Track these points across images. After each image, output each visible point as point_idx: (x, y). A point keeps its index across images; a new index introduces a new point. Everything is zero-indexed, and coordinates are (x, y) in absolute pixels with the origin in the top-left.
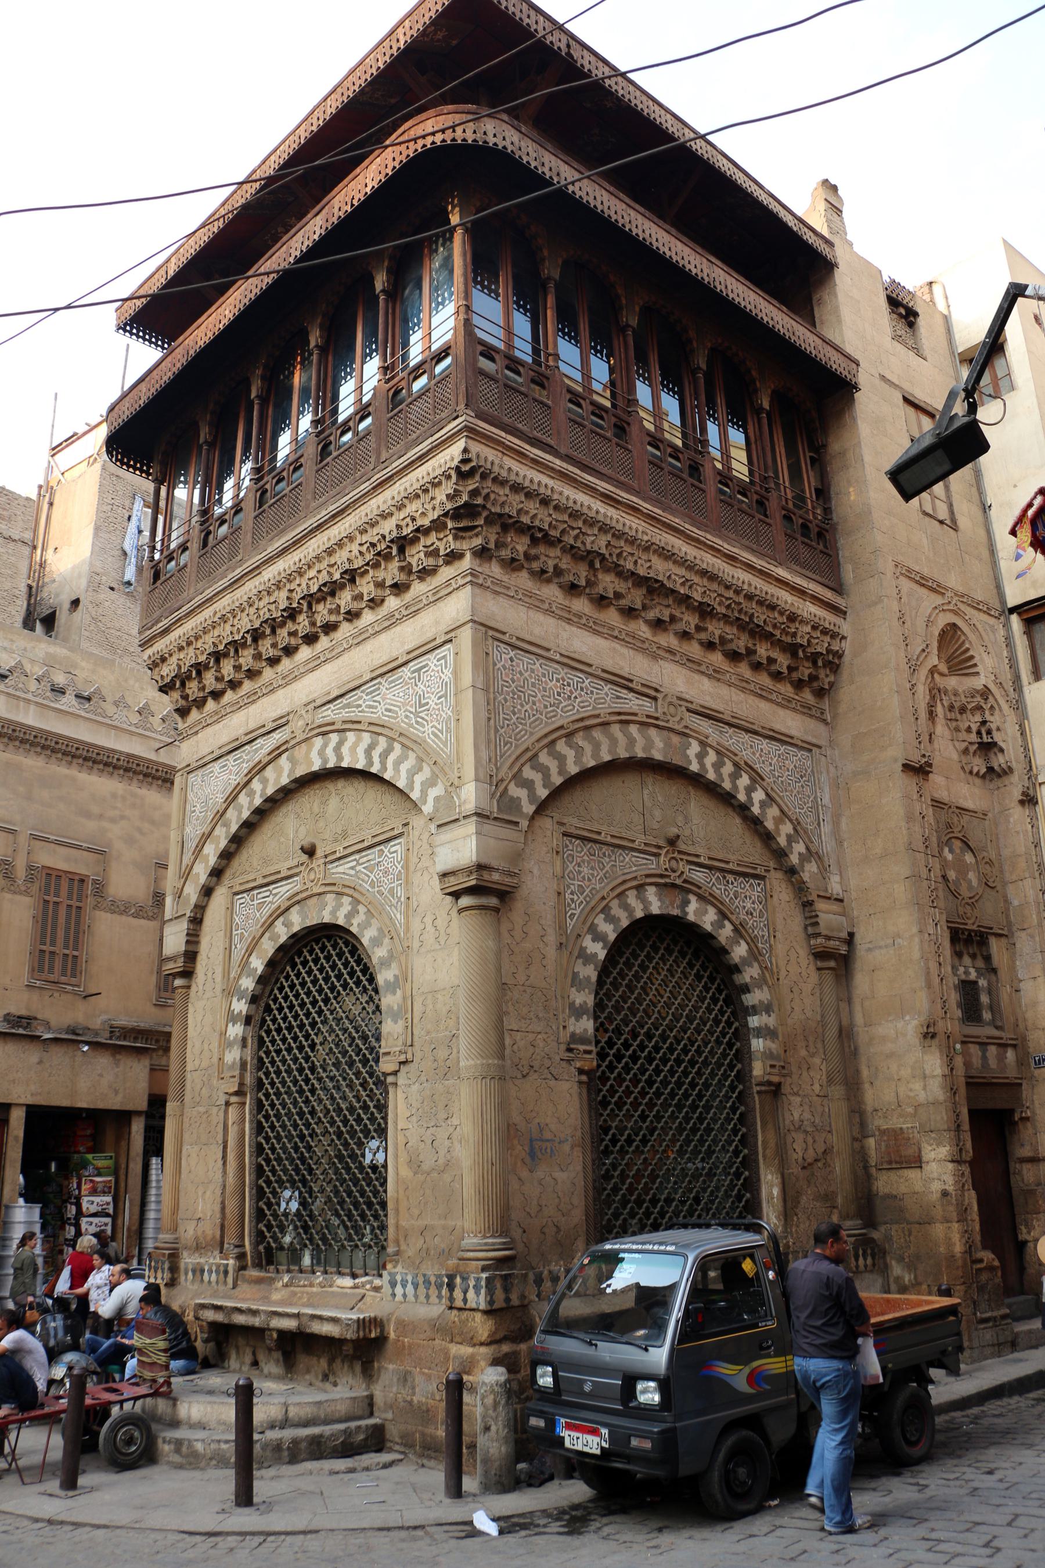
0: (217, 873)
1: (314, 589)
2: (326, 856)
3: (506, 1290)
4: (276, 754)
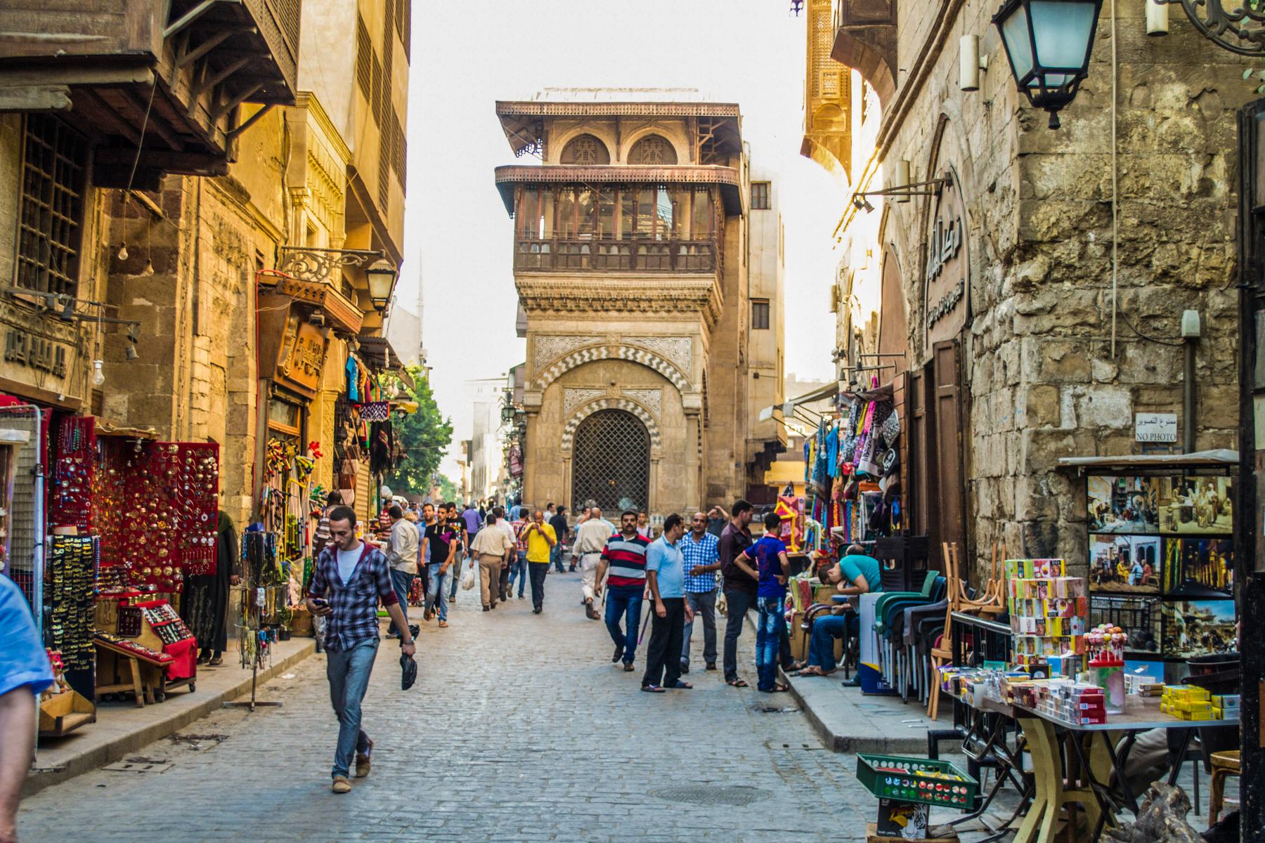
4: (598, 346)
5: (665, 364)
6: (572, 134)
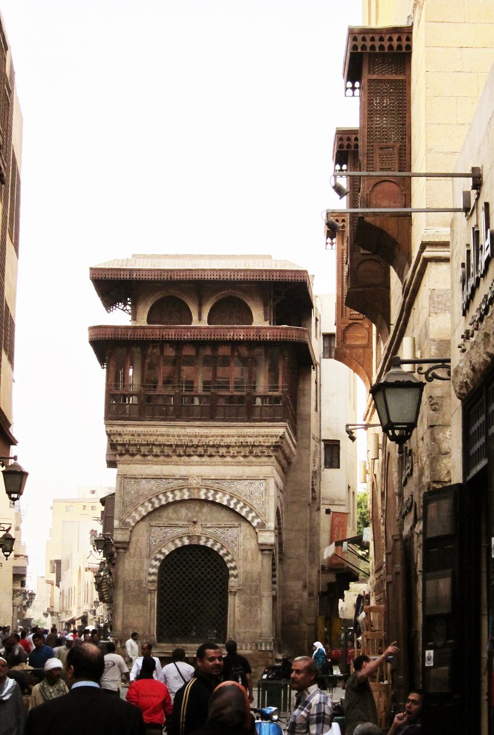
5: (242, 504)
6: (158, 296)
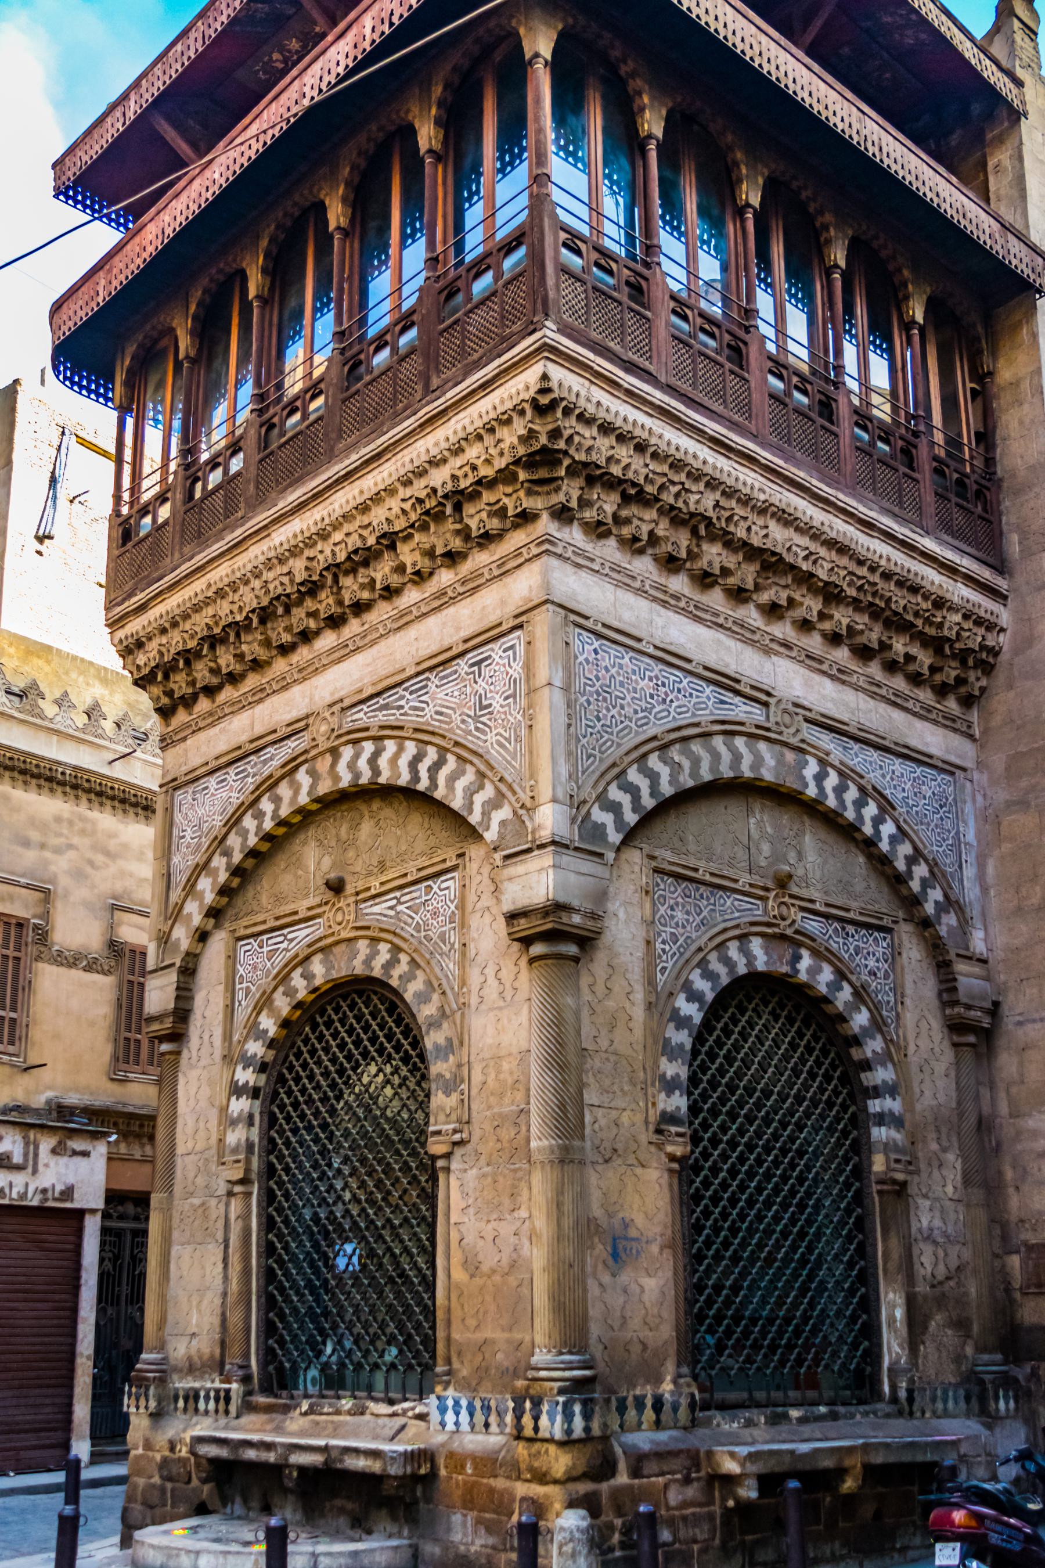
0: (214, 913)
1: (341, 557)
2: (357, 894)
3: (587, 1416)
4: (291, 767)
